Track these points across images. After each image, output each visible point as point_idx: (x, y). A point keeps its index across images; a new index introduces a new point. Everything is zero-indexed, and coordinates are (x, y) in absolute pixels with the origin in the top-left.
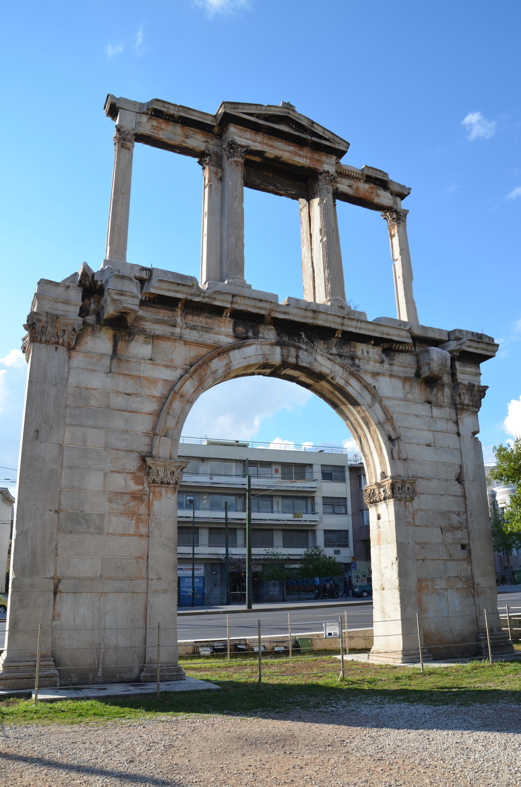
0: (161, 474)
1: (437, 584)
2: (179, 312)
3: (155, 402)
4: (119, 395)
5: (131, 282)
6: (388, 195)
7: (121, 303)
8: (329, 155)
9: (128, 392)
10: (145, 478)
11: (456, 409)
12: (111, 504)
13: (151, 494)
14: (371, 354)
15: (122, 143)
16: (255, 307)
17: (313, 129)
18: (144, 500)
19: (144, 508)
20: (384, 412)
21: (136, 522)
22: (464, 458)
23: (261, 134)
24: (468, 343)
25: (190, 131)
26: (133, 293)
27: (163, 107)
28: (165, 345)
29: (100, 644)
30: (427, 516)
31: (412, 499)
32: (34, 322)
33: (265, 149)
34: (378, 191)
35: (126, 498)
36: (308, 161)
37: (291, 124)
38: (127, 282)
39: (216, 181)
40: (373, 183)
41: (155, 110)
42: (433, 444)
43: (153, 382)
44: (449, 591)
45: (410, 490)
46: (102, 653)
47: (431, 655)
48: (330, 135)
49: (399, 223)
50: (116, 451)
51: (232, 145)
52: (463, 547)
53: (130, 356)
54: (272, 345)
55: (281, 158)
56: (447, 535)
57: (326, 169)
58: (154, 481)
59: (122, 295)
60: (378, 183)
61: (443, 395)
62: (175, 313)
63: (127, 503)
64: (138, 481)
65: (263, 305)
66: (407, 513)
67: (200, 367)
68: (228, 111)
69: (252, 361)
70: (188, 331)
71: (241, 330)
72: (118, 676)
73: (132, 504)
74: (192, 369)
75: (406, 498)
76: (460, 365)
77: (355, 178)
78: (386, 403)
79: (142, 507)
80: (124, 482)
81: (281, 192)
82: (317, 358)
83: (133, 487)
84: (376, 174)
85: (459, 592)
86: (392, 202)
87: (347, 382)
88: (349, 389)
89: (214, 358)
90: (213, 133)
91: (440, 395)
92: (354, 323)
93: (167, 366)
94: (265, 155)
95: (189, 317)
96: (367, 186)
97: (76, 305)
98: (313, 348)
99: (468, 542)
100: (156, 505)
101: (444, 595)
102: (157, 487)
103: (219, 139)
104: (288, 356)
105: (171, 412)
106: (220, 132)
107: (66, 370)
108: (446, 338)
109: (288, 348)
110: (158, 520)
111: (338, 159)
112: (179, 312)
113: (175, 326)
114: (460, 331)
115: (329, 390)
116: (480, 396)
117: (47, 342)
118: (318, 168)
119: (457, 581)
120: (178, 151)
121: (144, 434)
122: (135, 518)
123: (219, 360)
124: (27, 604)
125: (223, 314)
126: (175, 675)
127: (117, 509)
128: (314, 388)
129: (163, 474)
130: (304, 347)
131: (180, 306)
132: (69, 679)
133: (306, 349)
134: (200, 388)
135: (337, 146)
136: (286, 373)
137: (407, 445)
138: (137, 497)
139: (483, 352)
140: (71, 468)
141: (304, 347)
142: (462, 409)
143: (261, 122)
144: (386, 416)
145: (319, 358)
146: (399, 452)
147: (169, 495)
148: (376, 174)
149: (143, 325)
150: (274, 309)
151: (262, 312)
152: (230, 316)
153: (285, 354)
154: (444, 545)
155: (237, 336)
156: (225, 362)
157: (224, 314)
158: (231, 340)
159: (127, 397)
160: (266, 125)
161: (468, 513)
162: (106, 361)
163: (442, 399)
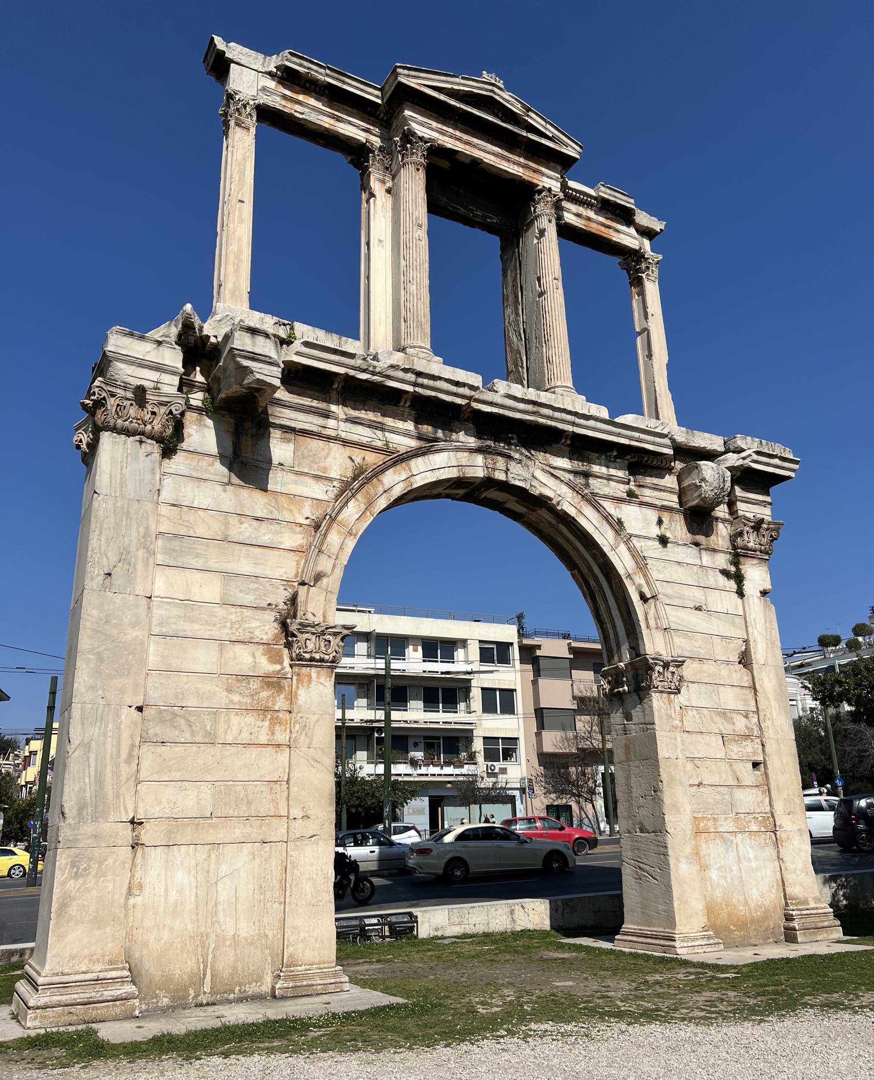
0: (310, 646)
1: (721, 825)
3: (300, 533)
4: (243, 520)
5: (268, 340)
6: (632, 231)
7: (252, 372)
8: (552, 164)
9: (259, 514)
10: (286, 651)
12: (230, 695)
13: (295, 678)
15: (237, 119)
18: (284, 687)
19: (283, 700)
20: (633, 556)
21: (271, 723)
22: (750, 629)
23: (452, 122)
24: (755, 457)
26: (270, 358)
27: (301, 65)
28: (315, 444)
29: (207, 935)
30: (701, 717)
31: (678, 691)
32: (104, 397)
33: (459, 147)
35: (255, 685)
36: (521, 170)
37: (496, 111)
38: (260, 339)
39: (383, 193)
40: (611, 212)
42: (704, 607)
44: (739, 836)
45: (675, 676)
46: (211, 950)
47: (721, 941)
49: (648, 275)
50: (239, 609)
52: (755, 765)
53: (261, 460)
55: (480, 163)
56: (731, 747)
57: (547, 186)
58: (300, 658)
59: (253, 359)
60: (618, 212)
62: (328, 397)
63: (257, 693)
66: (673, 712)
67: (369, 480)
70: (349, 425)
72: (237, 989)
73: (264, 694)
74: (356, 484)
75: (670, 688)
78: (636, 543)
79: (279, 699)
80: (251, 659)
81: (477, 220)
82: (535, 474)
83: (266, 666)
84: (615, 197)
85: (753, 837)
89: (387, 468)
90: (377, 117)
92: (591, 423)
94: (457, 157)
97: (174, 373)
98: (529, 458)
99: (762, 759)
100: (303, 696)
101: (732, 842)
102: (304, 666)
103: (387, 128)
104: (494, 469)
105: (324, 548)
106: (389, 115)
107: (158, 478)
108: (723, 449)
109: (495, 457)
110: (305, 719)
111: (563, 171)
115: (550, 523)
116: (771, 536)
118: (535, 181)
119: (750, 822)
120: (322, 142)
121: (283, 583)
122: (269, 717)
123: (395, 472)
124: (85, 869)
125: (400, 402)
126: (331, 984)
127: (240, 703)
128: (526, 519)
129: (313, 645)
130: (517, 456)
131: (335, 386)
132: (155, 1000)
133: (520, 460)
134: (369, 513)
136: (488, 496)
137: (667, 607)
138: (273, 682)
141: (517, 456)
143: (453, 102)
144: (636, 562)
145: (539, 474)
146: (657, 618)
147: (322, 680)
148: (615, 197)
149: (280, 412)
150: (477, 397)
151: (459, 401)
152: (409, 406)
153: (489, 466)
154: (728, 762)
157: (402, 403)
159: (255, 523)
160: (460, 108)
161: (761, 714)
163: (715, 540)
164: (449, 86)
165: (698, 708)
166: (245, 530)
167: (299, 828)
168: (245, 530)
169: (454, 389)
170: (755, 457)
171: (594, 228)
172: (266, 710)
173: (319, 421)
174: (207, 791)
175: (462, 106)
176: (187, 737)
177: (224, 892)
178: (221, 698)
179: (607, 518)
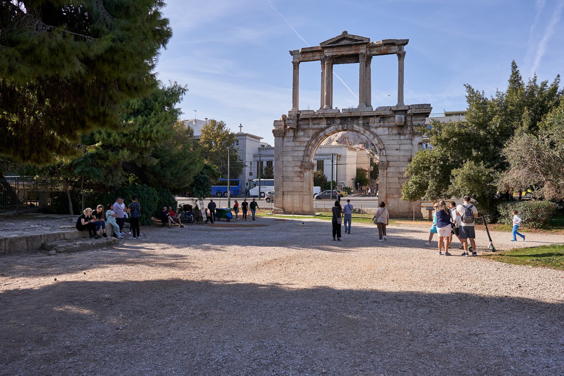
2: (310, 120)
6: (396, 47)
11: (412, 135)
14: (375, 121)
16: (330, 115)
17: (355, 38)
24: (415, 110)
25: (315, 54)
28: (307, 131)
31: (386, 169)
33: (338, 53)
34: (391, 48)
35: (298, 173)
40: (388, 45)
41: (303, 52)
43: (304, 142)
48: (361, 38)
51: (326, 57)
54: (339, 125)
57: (361, 52)
61: (407, 130)
64: (301, 168)
65: (333, 114)
67: (317, 135)
68: (322, 46)
69: (332, 131)
71: (329, 122)
76: (415, 118)
77: (379, 46)
83: (300, 170)
86: (397, 50)
87: (365, 133)
88: (365, 134)
91: (405, 130)
93: (307, 137)
95: (313, 121)
96: (385, 48)
100: (305, 174)
112: (310, 120)
113: (309, 125)
114: (413, 105)
117: (278, 136)
135: (364, 42)
138: (301, 172)
139: (424, 112)
140: (285, 166)
142: (414, 135)
143: (334, 45)
145: (355, 126)
146: (383, 154)
151: (333, 116)
155: (327, 124)
156: (324, 133)
158: (326, 126)
162: (292, 138)
164: (333, 41)
165: (392, 172)
166: (296, 149)
167: (305, 193)
168: (296, 149)
169: (331, 114)
170: (415, 110)
171: (382, 52)
172: (300, 176)
173: (308, 126)
174: (292, 188)
175: (336, 45)
176: (289, 180)
177: (295, 201)
178: (293, 175)
179: (372, 133)
